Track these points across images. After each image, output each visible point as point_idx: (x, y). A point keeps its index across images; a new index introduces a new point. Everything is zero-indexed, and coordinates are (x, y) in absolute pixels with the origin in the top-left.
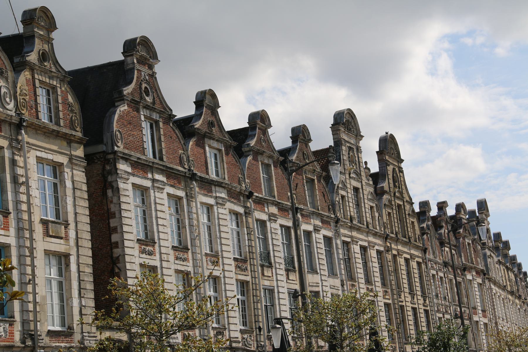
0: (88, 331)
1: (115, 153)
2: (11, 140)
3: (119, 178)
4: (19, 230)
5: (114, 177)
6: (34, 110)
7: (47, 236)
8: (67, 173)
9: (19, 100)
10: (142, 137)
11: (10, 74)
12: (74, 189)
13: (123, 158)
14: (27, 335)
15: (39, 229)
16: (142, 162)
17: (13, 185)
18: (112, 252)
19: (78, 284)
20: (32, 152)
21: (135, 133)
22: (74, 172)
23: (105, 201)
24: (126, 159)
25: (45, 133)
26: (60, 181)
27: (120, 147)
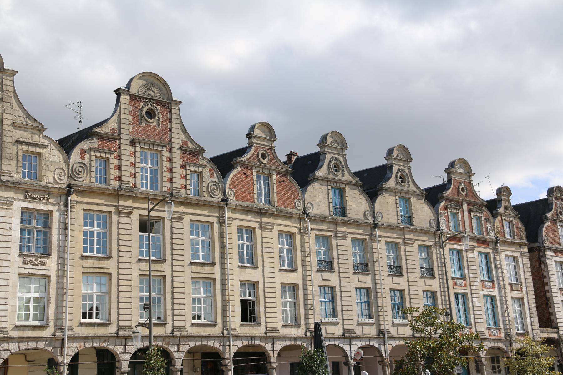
1: (544, 247)
2: (493, 249)
3: (547, 259)
4: (499, 289)
5: (544, 258)
10: (559, 237)
11: (491, 220)
12: (524, 267)
13: (548, 249)
15: (508, 288)
16: (560, 249)
18: (546, 295)
21: (555, 235)
22: (523, 259)
23: (541, 270)
24: (550, 249)
26: (517, 264)
27: (547, 244)
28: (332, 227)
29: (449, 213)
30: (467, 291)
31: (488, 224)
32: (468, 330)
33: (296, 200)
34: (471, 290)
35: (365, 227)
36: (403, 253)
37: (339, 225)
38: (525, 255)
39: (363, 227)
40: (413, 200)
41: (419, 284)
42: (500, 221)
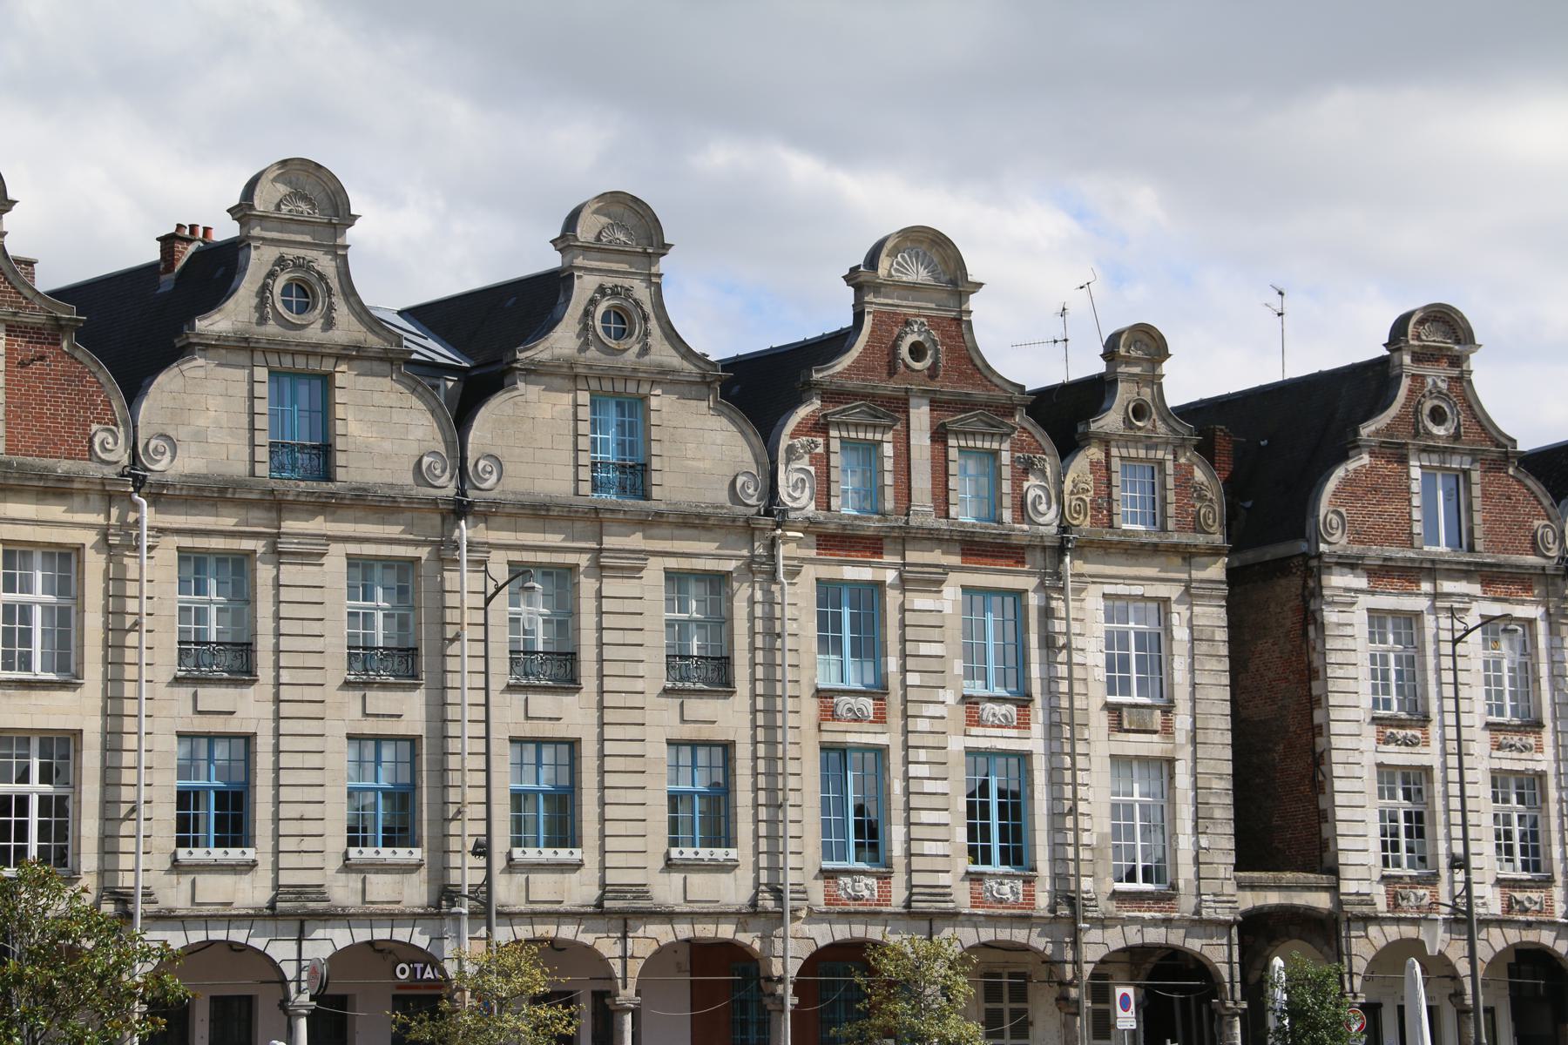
0: (1214, 891)
1: (1320, 556)
2: (1043, 576)
3: (1330, 604)
4: (1053, 729)
5: (1318, 602)
6: (1105, 512)
7: (1119, 731)
8: (1179, 613)
9: (1066, 504)
10: (1410, 514)
11: (1050, 464)
12: (1193, 640)
13: (1338, 564)
14: (1061, 898)
15: (1100, 721)
16: (1400, 564)
17: (1045, 651)
18: (1314, 743)
19: (1192, 809)
20: (1091, 587)
21: (1389, 508)
22: (1195, 608)
23: (1305, 646)
24: (1350, 564)
25: (1126, 550)
26: (1166, 629)
27: (1337, 542)
28: (258, 521)
29: (835, 445)
30: (888, 737)
31: (1031, 477)
32: (873, 882)
33: (95, 427)
34: (906, 732)
35: (415, 514)
36: (587, 606)
37: (292, 511)
38: (1208, 592)
39: (408, 515)
40: (660, 402)
41: (648, 717)
42: (1099, 462)
